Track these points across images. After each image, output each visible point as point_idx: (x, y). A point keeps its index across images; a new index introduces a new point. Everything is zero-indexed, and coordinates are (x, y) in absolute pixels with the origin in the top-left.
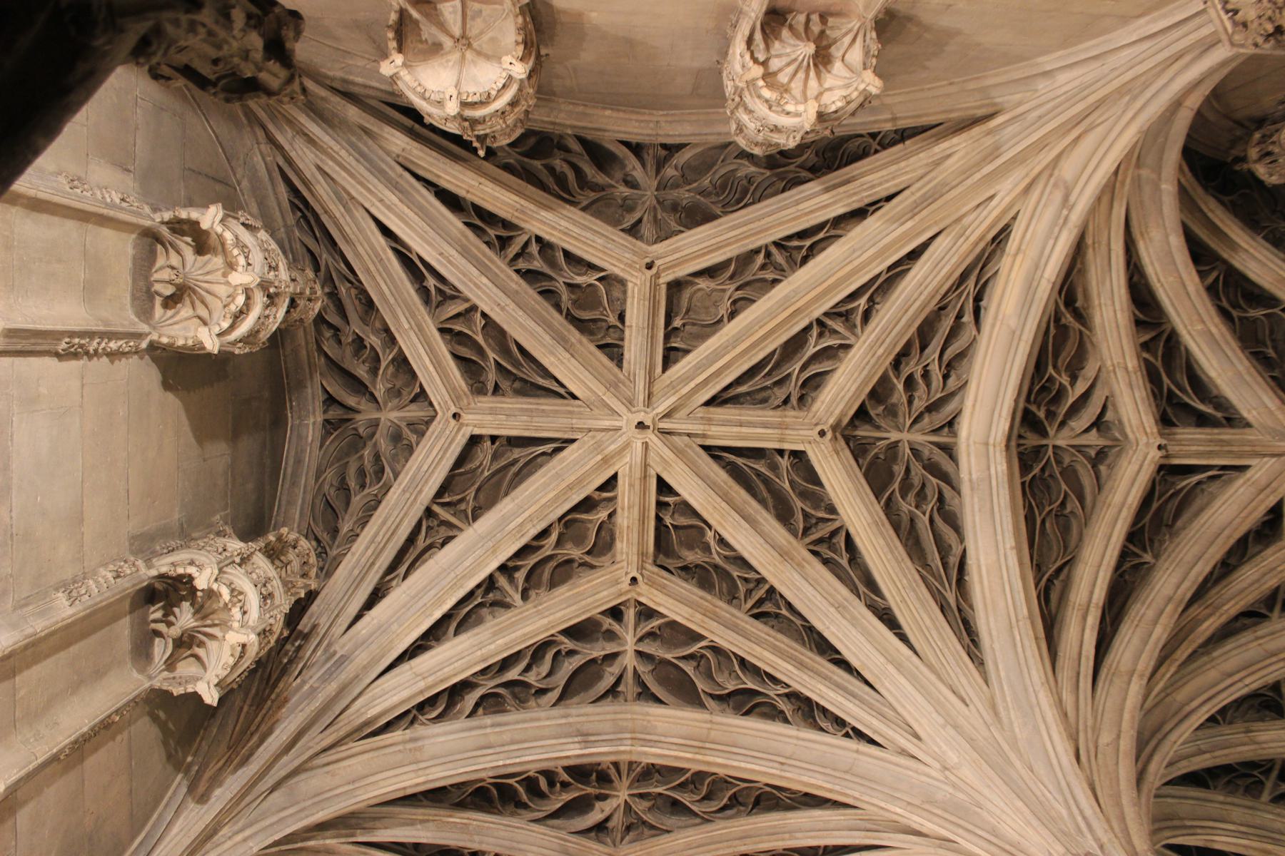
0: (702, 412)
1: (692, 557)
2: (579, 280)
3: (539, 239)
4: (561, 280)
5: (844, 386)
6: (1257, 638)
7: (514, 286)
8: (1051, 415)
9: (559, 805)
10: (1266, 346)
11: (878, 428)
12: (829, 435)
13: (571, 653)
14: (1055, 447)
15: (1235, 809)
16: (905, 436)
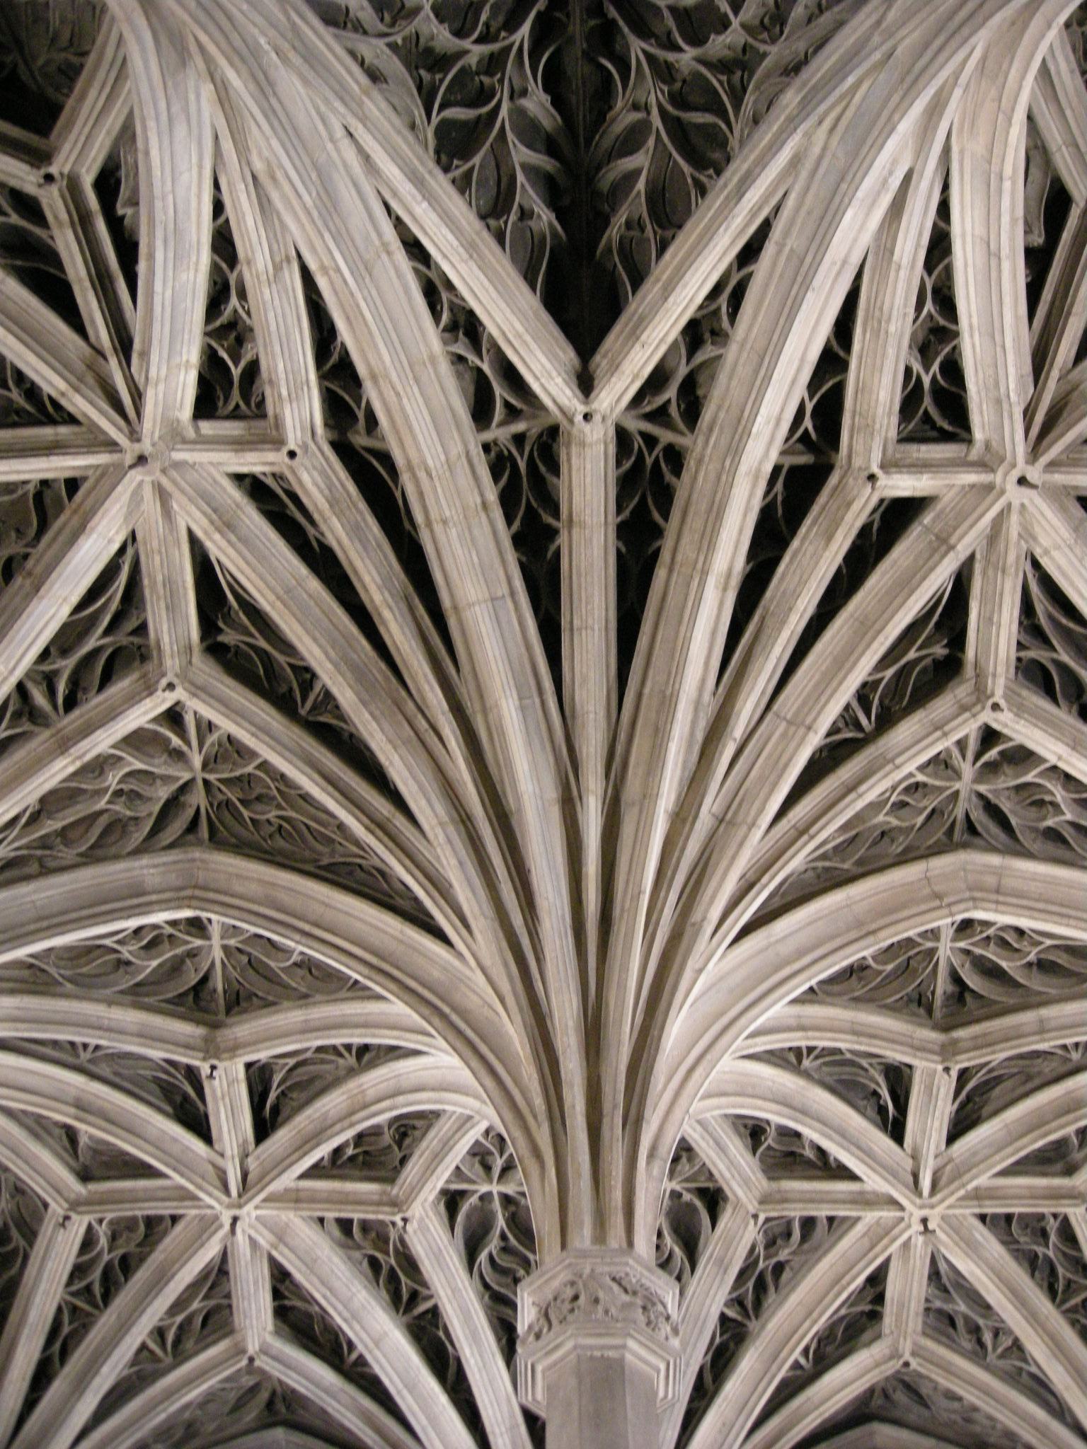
0: (216, 1146)
1: (387, 1139)
2: (103, 1242)
3: (70, 1282)
4: (106, 1257)
5: (161, 1038)
6: (429, 524)
7: (114, 1317)
8: (166, 779)
9: (677, 1250)
10: (25, 494)
11: (213, 964)
12: (215, 1062)
13: (503, 1237)
14: (205, 766)
15: (681, 550)
16: (216, 941)
